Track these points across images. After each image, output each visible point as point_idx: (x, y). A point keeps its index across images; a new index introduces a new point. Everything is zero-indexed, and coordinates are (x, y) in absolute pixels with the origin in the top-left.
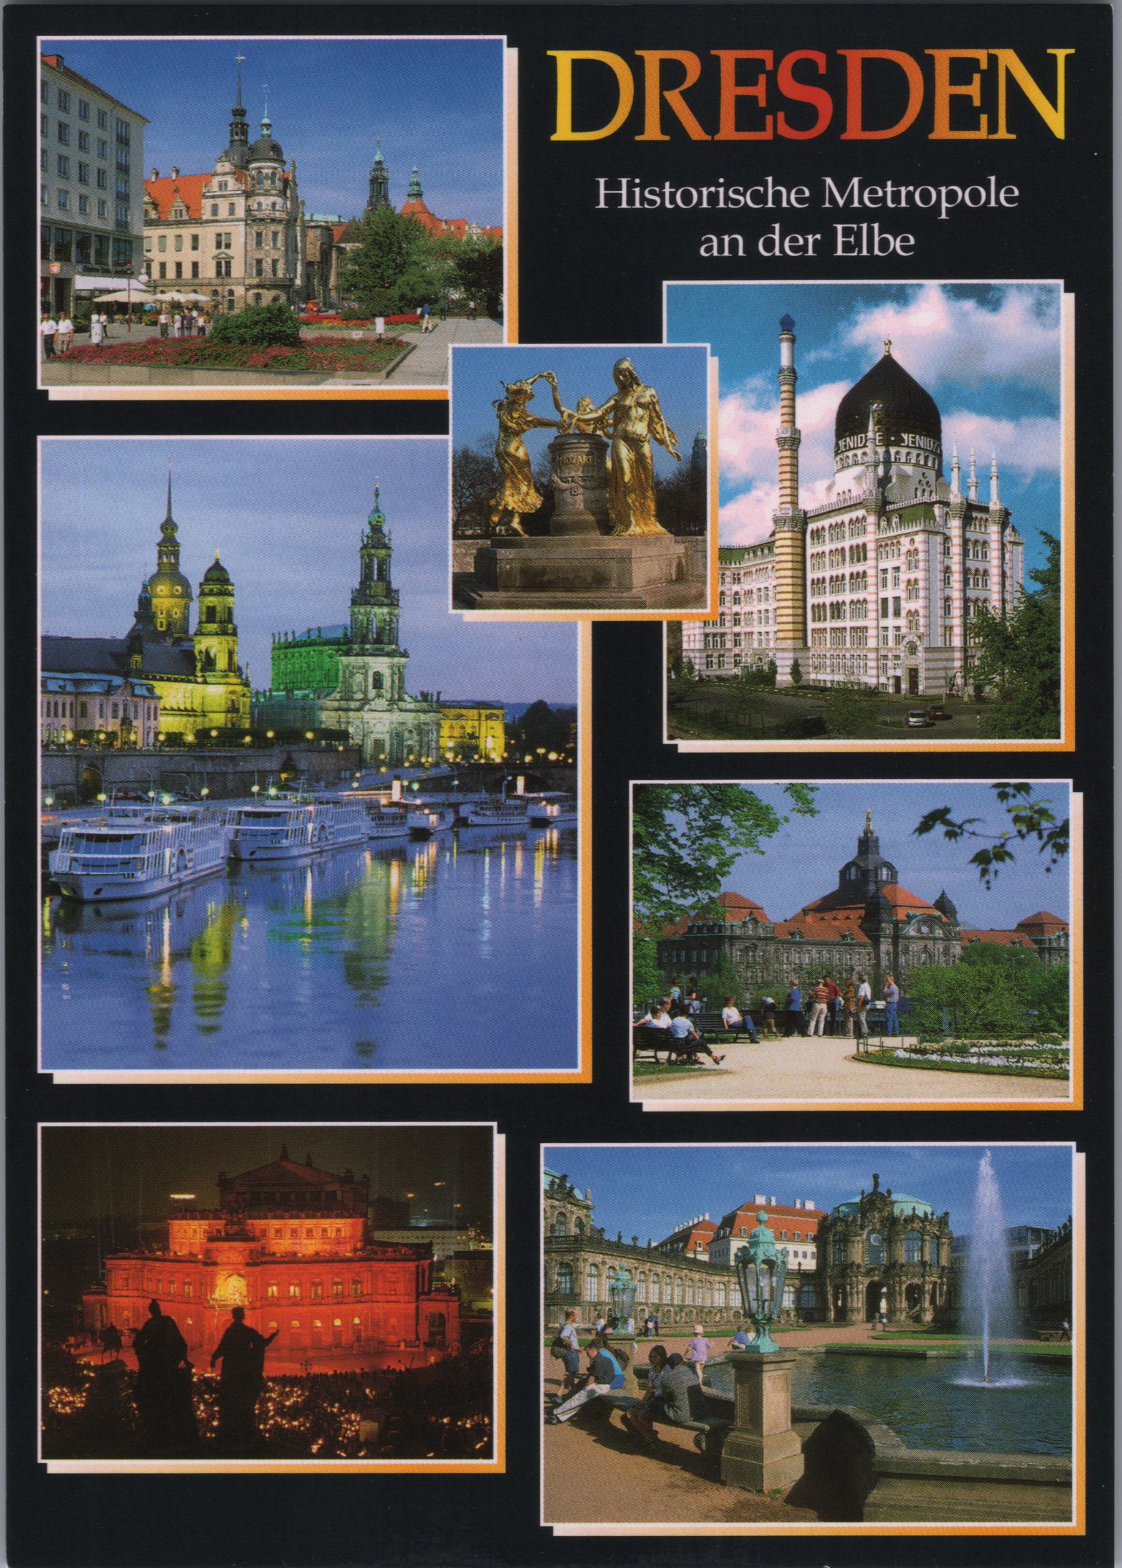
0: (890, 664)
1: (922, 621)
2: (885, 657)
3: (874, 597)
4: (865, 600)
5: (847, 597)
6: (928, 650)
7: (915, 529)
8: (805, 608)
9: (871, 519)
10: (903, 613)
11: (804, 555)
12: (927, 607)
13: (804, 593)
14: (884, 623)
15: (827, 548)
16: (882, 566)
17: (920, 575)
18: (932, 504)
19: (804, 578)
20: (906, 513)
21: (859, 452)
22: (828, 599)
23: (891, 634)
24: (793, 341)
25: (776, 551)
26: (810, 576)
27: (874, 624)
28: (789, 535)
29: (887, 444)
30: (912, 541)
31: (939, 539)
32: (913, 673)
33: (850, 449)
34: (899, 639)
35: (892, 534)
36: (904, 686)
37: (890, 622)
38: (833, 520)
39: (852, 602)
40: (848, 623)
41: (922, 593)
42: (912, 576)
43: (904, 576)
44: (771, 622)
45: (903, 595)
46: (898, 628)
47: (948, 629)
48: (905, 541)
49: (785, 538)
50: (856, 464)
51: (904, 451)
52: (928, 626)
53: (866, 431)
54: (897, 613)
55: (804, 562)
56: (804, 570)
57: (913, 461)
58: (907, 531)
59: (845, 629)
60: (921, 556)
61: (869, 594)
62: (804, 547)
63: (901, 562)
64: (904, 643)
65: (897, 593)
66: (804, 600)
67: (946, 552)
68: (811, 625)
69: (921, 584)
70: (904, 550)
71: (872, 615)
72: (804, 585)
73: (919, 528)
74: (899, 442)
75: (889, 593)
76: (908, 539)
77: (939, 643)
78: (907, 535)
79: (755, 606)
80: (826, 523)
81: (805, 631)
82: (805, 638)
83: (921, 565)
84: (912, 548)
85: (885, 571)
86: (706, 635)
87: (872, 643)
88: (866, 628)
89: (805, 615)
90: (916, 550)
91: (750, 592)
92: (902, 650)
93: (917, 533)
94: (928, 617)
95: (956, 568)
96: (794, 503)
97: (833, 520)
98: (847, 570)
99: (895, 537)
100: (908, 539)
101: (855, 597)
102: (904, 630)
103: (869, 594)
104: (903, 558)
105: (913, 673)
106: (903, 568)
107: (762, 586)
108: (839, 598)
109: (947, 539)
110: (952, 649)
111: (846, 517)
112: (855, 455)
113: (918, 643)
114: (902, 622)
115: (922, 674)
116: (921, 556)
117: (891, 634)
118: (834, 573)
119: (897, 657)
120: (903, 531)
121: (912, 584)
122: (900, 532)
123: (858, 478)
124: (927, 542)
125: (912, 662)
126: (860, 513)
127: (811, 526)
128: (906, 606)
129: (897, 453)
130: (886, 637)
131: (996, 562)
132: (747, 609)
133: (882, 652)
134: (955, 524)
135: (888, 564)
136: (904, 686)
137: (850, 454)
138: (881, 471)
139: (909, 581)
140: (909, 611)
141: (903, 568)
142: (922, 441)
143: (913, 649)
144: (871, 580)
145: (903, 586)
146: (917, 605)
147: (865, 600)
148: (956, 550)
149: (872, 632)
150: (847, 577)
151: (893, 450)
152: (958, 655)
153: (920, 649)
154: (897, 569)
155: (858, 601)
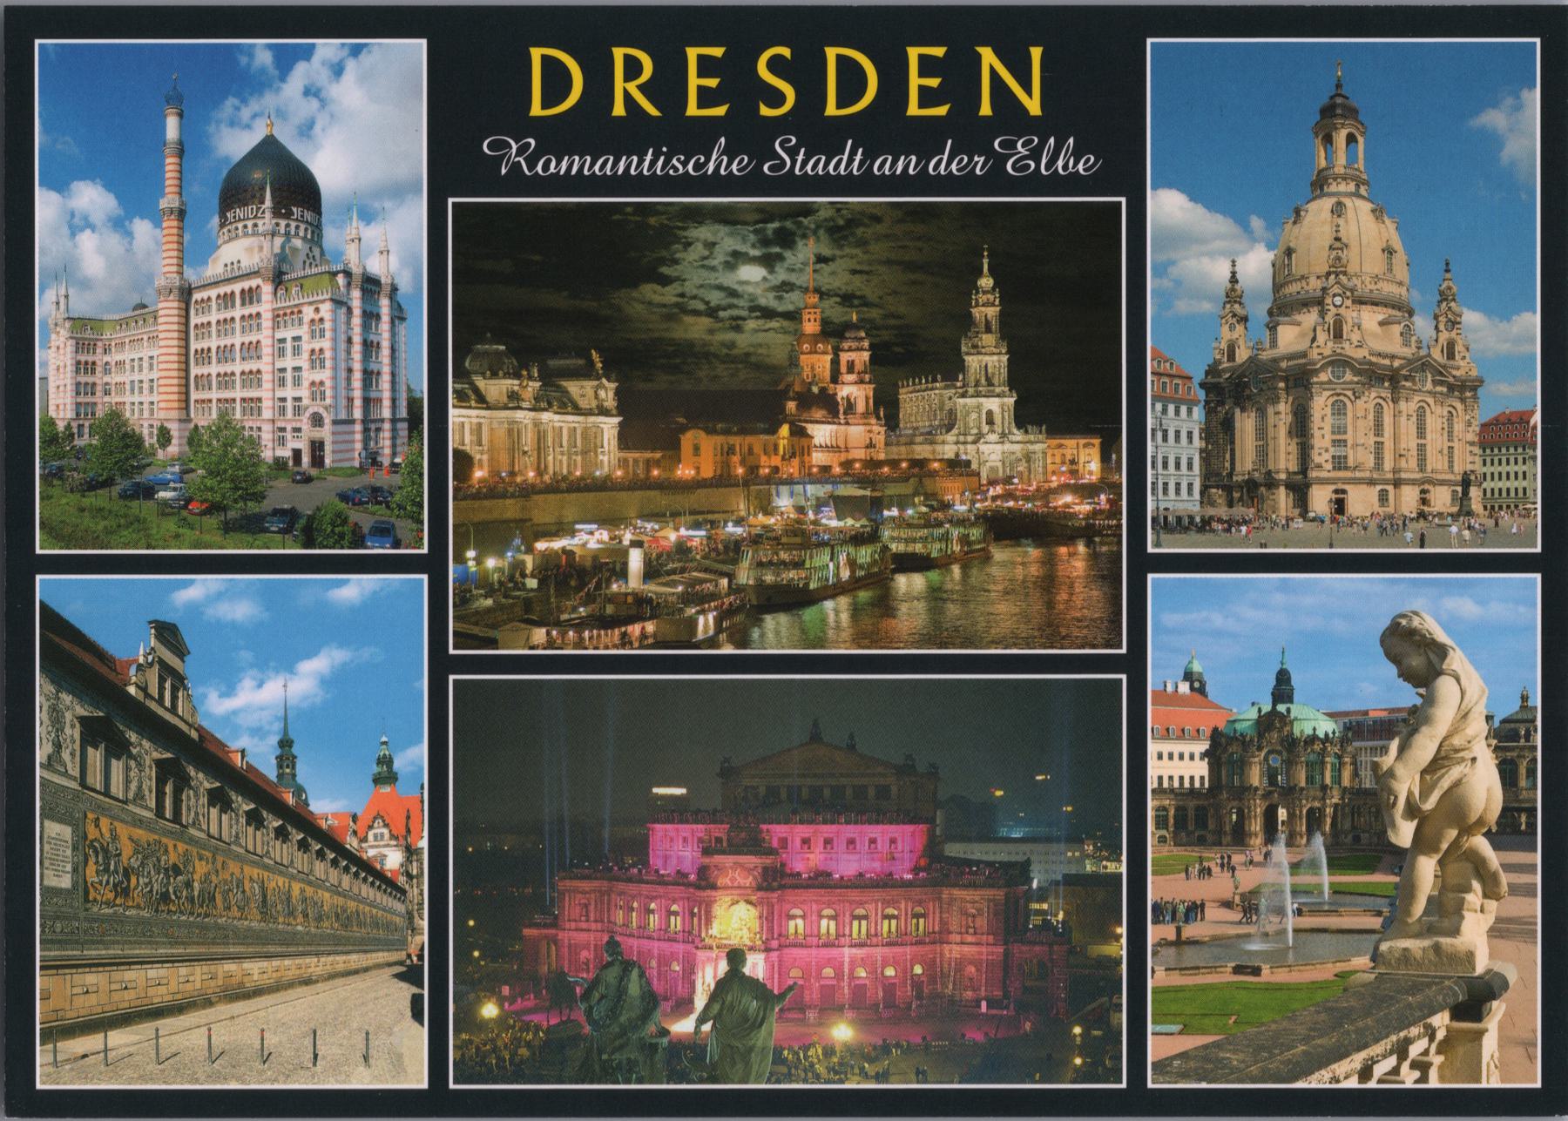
0: (289, 436)
1: (329, 393)
2: (283, 430)
3: (270, 368)
4: (259, 372)
5: (237, 367)
6: (335, 422)
8: (187, 378)
9: (267, 289)
10: (306, 384)
11: (187, 324)
12: (334, 378)
13: (187, 363)
14: (279, 394)
15: (214, 317)
16: (279, 335)
17: (326, 344)
18: (335, 274)
19: (187, 347)
20: (307, 283)
21: (250, 223)
22: (214, 369)
23: (289, 404)
24: (181, 115)
25: (161, 320)
26: (194, 346)
27: (270, 395)
28: (176, 304)
29: (276, 213)
30: (317, 310)
31: (344, 310)
32: (317, 447)
34: (297, 411)
36: (306, 459)
37: (289, 392)
38: (223, 290)
39: (243, 373)
40: (238, 394)
41: (328, 364)
42: (317, 346)
43: (306, 346)
44: (145, 392)
45: (305, 365)
46: (298, 399)
47: (350, 400)
48: (308, 313)
49: (168, 309)
50: (246, 235)
51: (293, 224)
52: (335, 397)
53: (263, 202)
54: (297, 382)
55: (187, 332)
56: (187, 340)
57: (301, 234)
59: (234, 400)
60: (327, 325)
61: (264, 365)
62: (187, 317)
63: (303, 331)
64: (307, 414)
65: (297, 363)
66: (187, 371)
67: (348, 322)
68: (194, 396)
69: (328, 354)
70: (306, 319)
71: (267, 385)
72: (187, 355)
74: (289, 215)
75: (288, 362)
76: (312, 308)
77: (343, 416)
78: (310, 303)
79: (125, 378)
80: (213, 293)
81: (187, 401)
82: (187, 408)
83: (328, 334)
84: (317, 317)
85: (283, 341)
86: (78, 404)
87: (267, 414)
88: (259, 400)
89: (187, 385)
90: (321, 320)
91: (120, 364)
92: (305, 424)
93: (323, 301)
94: (335, 388)
95: (357, 339)
96: (180, 273)
97: (223, 290)
98: (237, 340)
100: (312, 308)
101: (223, 368)
102: (306, 402)
103: (264, 365)
104: (305, 328)
105: (317, 447)
106: (305, 338)
107: (136, 356)
108: (228, 368)
109: (350, 310)
110: (352, 422)
111: (237, 288)
112: (245, 227)
113: (325, 415)
114: (304, 393)
115: (328, 448)
116: (327, 325)
117: (289, 404)
118: (247, 340)
119: (298, 430)
121: (316, 359)
123: (249, 250)
124: (334, 312)
125: (318, 434)
126: (254, 283)
127: (197, 296)
128: (308, 376)
129: (288, 226)
130: (283, 410)
131: (386, 335)
132: (119, 379)
133: (279, 424)
134: (356, 294)
135: (288, 334)
136: (306, 459)
137: (240, 225)
138: (278, 241)
139: (313, 351)
140: (313, 384)
141: (305, 338)
142: (308, 215)
143: (317, 420)
144: (266, 350)
145: (306, 356)
146: (325, 375)
147: (259, 372)
148: (357, 320)
149: (267, 404)
150: (238, 347)
151: (283, 223)
152: (358, 427)
153: (327, 421)
154: (297, 339)
155: (251, 372)
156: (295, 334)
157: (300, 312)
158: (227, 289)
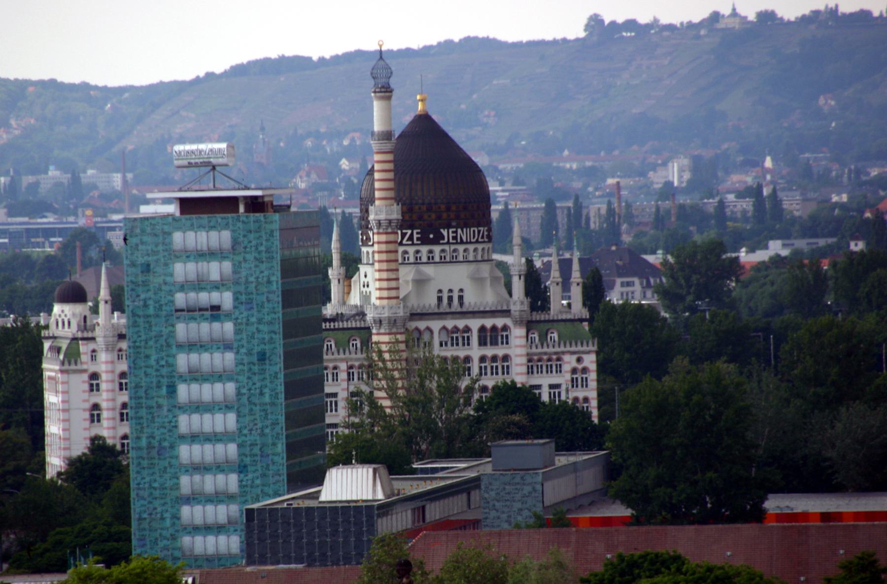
7: (585, 348)
21: (471, 247)
33: (462, 242)
35: (551, 350)
48: (569, 362)
58: (573, 349)
70: (567, 368)
73: (591, 348)
76: (575, 357)
84: (580, 367)
90: (585, 370)
93: (589, 352)
99: (556, 353)
100: (575, 357)
120: (568, 349)
122: (562, 349)
156: (555, 380)
157: (559, 359)
158: (461, 323)
